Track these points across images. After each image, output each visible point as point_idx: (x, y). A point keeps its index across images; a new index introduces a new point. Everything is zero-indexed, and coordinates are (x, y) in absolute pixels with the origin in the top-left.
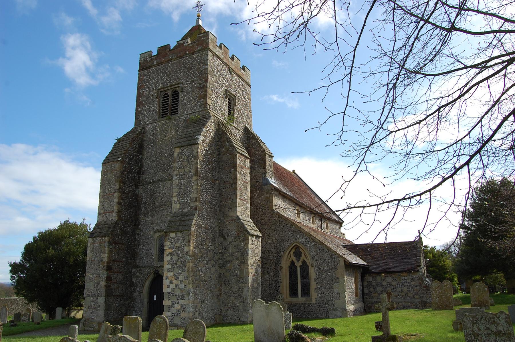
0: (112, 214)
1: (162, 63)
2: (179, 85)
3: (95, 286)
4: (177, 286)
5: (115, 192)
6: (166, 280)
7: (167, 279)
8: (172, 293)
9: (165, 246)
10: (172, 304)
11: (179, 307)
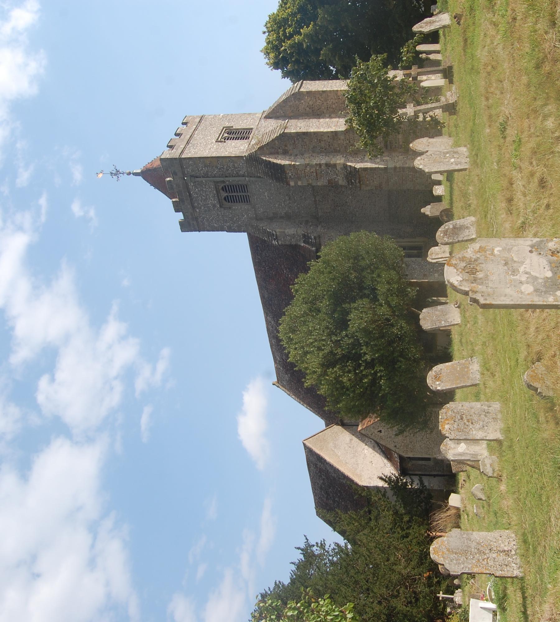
2: (225, 129)
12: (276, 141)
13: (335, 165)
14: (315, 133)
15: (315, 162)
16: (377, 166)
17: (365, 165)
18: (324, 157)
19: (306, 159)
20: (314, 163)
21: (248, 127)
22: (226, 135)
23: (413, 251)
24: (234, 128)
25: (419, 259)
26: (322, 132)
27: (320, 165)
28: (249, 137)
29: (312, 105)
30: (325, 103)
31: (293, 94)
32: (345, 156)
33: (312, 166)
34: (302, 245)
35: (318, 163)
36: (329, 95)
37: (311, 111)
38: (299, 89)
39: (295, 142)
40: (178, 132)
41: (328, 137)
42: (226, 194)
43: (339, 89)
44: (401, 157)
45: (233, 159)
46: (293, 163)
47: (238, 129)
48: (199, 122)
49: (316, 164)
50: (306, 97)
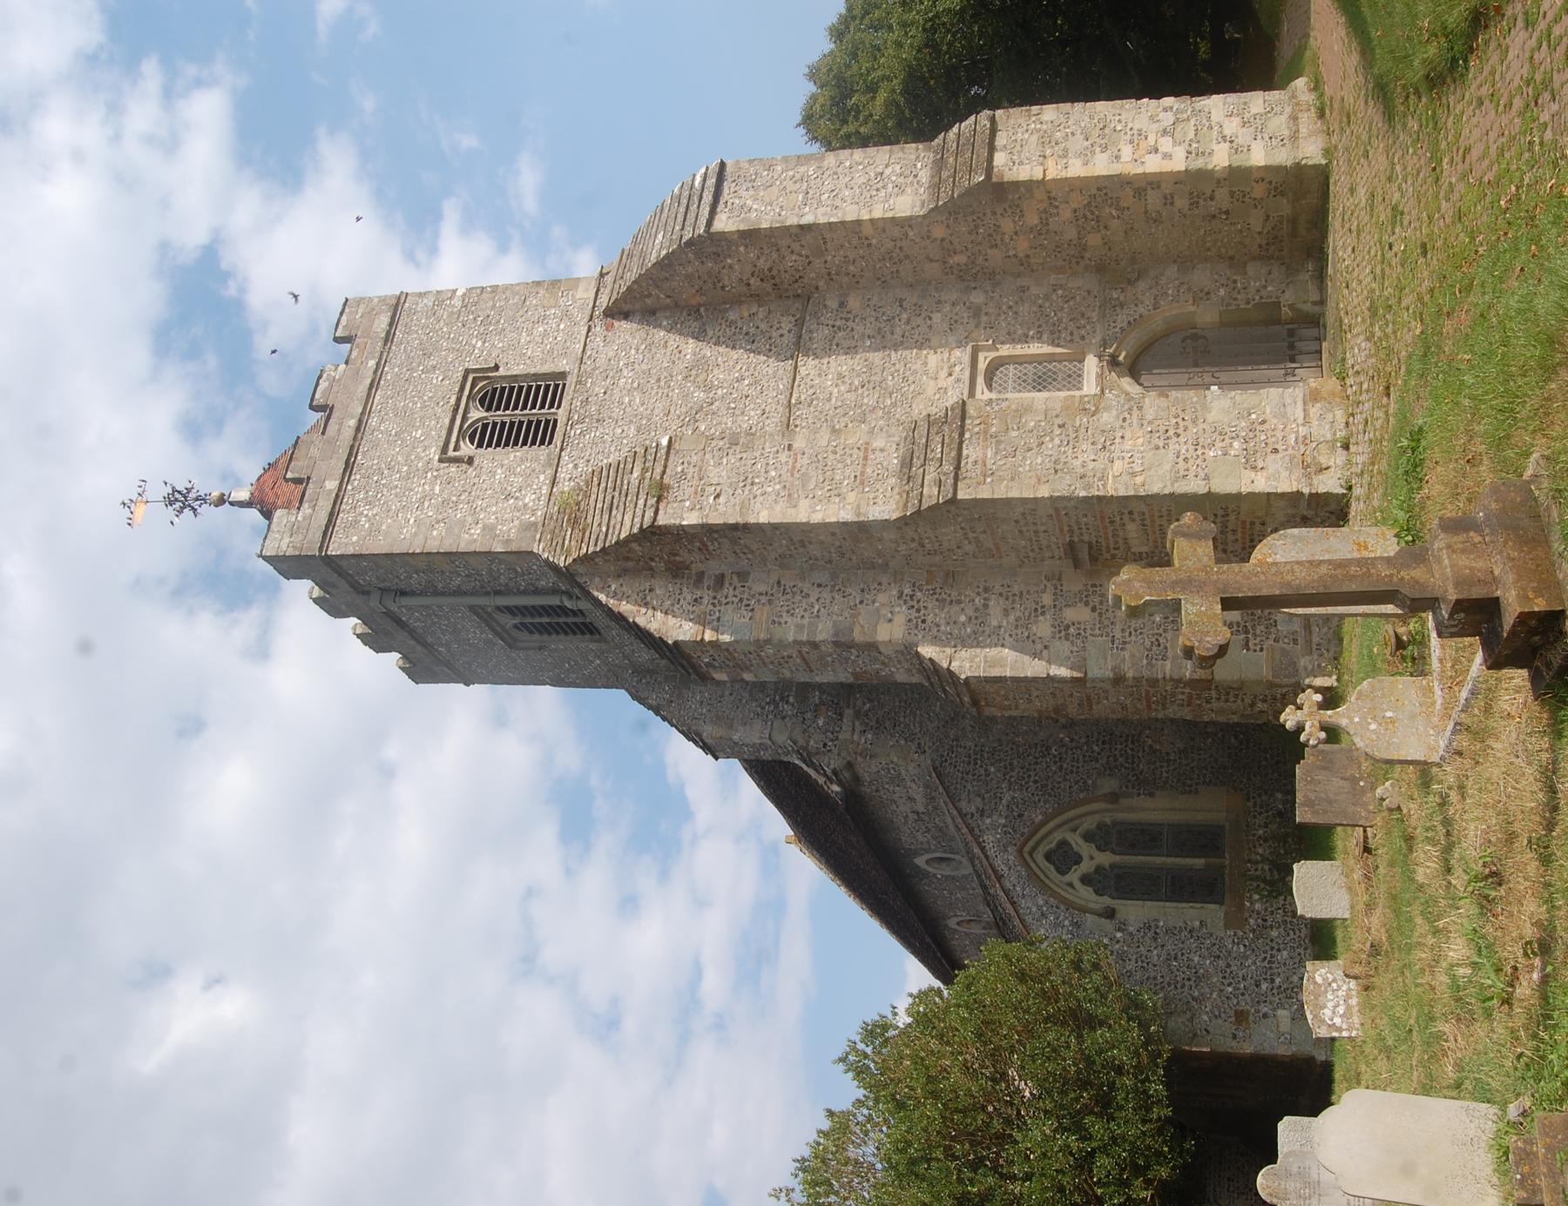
0: (874, 451)
1: (350, 455)
3: (1161, 445)
4: (1165, 132)
9: (1032, 176)
10: (1225, 141)
11: (1236, 121)
12: (634, 546)
13: (872, 647)
14: (775, 527)
15: (791, 631)
16: (1034, 668)
17: (992, 664)
18: (826, 595)
19: (758, 614)
20: (790, 640)
21: (547, 368)
22: (477, 414)
23: (1189, 861)
24: (502, 372)
25: (1213, 914)
26: (807, 524)
27: (815, 645)
28: (556, 421)
29: (770, 270)
30: (817, 263)
31: (690, 243)
32: (907, 591)
33: (782, 645)
34: (797, 762)
35: (804, 638)
36: (828, 236)
37: (768, 286)
38: (709, 223)
39: (705, 545)
41: (833, 534)
42: (517, 620)
45: (505, 557)
46: (709, 636)
47: (515, 378)
48: (386, 341)
49: (796, 642)
50: (742, 249)
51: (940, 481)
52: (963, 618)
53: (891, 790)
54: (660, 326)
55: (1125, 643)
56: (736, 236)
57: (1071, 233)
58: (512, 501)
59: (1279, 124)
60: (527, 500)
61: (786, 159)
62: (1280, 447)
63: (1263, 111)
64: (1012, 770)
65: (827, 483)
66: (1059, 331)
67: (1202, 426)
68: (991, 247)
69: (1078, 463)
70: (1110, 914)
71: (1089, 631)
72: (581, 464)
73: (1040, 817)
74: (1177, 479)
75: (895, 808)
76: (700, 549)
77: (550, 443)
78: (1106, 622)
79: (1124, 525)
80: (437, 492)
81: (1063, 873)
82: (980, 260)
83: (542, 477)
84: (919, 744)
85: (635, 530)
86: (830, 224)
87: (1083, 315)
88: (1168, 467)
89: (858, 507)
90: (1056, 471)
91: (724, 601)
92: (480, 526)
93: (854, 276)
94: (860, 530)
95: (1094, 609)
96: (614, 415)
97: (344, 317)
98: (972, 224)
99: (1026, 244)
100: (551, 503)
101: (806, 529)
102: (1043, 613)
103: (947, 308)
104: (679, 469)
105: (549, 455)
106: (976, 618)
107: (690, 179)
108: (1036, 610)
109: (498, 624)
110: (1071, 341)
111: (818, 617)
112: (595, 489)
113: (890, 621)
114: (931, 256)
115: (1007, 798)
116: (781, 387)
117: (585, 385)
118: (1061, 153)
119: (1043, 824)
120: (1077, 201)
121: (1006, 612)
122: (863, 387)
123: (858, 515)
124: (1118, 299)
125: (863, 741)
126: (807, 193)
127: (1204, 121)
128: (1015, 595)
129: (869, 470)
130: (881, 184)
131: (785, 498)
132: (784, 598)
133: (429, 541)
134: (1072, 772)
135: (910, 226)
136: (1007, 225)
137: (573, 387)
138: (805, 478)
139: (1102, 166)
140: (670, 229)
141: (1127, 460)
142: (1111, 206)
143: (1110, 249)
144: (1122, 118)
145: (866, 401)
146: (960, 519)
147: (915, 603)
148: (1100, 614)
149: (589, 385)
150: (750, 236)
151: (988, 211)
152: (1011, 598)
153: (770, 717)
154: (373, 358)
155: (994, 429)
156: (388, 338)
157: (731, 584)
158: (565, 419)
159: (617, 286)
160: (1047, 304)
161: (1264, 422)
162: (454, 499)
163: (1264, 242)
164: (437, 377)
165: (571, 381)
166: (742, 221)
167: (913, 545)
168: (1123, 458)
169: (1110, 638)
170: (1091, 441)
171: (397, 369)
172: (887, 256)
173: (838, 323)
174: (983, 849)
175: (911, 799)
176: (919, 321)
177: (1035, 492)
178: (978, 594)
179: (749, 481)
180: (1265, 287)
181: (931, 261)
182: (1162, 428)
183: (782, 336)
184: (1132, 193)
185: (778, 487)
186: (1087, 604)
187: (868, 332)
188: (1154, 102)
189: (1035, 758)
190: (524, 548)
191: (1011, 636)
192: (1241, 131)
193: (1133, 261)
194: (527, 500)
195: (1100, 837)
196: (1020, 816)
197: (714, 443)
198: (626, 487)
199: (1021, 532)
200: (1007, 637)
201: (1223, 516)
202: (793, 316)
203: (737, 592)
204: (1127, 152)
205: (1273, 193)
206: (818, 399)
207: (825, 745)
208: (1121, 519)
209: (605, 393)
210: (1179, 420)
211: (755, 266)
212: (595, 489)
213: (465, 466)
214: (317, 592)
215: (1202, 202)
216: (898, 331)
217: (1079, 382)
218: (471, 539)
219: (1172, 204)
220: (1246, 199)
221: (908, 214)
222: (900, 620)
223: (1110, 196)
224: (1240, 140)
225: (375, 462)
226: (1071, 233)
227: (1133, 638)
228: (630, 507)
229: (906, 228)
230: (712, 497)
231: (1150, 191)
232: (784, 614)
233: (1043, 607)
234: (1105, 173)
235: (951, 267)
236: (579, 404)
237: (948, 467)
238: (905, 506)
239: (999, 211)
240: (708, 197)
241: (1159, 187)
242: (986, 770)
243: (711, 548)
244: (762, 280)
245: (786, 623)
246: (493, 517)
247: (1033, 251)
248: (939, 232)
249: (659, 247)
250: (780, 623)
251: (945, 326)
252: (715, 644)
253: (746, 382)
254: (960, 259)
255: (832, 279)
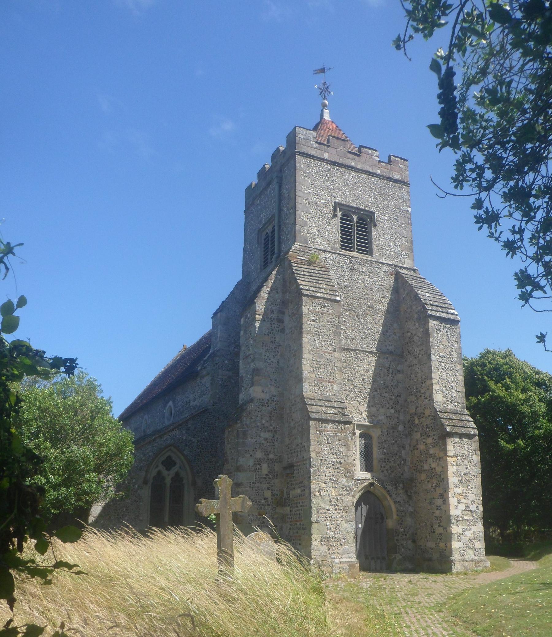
0: (332, 385)
3: (332, 503)
4: (467, 507)
5: (334, 351)
6: (452, 499)
7: (453, 497)
8: (461, 517)
9: (449, 451)
11: (472, 536)
12: (295, 286)
14: (301, 345)
21: (374, 247)
28: (351, 251)
29: (414, 341)
30: (415, 361)
31: (424, 308)
32: (275, 399)
40: (363, 150)
42: (269, 234)
43: (434, 381)
44: (268, 494)
45: (294, 230)
47: (371, 233)
50: (422, 330)
51: (318, 413)
52: (264, 422)
53: (199, 391)
54: (391, 295)
55: (253, 488)
56: (427, 327)
57: (426, 467)
58: (317, 233)
59: (470, 555)
60: (317, 239)
61: (460, 348)
62: (330, 552)
63: (476, 547)
64: (206, 442)
65: (319, 366)
66: (385, 462)
67: (340, 520)
68: (421, 434)
69: (325, 469)
70: (145, 482)
71: (258, 473)
72: (333, 262)
73: (186, 454)
74: (317, 510)
75: (192, 393)
76: (293, 313)
77: (342, 249)
78: (261, 480)
79: (300, 488)
80: (322, 201)
81: (163, 463)
82: (416, 429)
83: (327, 246)
84: (217, 403)
85: (301, 286)
86: (431, 367)
87: (392, 472)
88: (322, 505)
89: (309, 379)
90: (321, 460)
91: (272, 323)
92: (307, 220)
93: (411, 376)
94: (299, 379)
95: (267, 475)
96: (353, 276)
97: (399, 159)
98: (430, 426)
99: (422, 448)
100: (316, 250)
101: (300, 358)
102: (265, 454)
103: (396, 415)
104: (326, 305)
105: (337, 248)
106: (264, 427)
107: (453, 308)
108: (267, 452)
109: (268, 226)
110: (381, 467)
111: (265, 362)
112: (319, 269)
113: (263, 392)
114: (418, 409)
115: (194, 440)
116: (364, 346)
117: (367, 263)
118: (459, 463)
119: (183, 455)
120: (439, 469)
121: (266, 439)
122: (363, 380)
123: (305, 379)
124: (399, 486)
125: (219, 380)
126: (445, 357)
127: (472, 523)
128: (273, 443)
129: (324, 383)
130: (448, 388)
131: (313, 349)
132: (273, 347)
133: (300, 198)
134: (205, 466)
135: (429, 400)
136: (429, 441)
137: (365, 258)
138: (321, 357)
139: (453, 480)
140: (431, 299)
141: (326, 489)
142: (437, 484)
143: (420, 483)
144: (474, 489)
145: (357, 381)
146: (303, 421)
147: (270, 402)
148: (265, 478)
149: (366, 265)
150: (427, 333)
151: (435, 433)
152: (272, 441)
153: (229, 341)
154: (381, 172)
155: (339, 435)
156: (390, 179)
157: (279, 326)
158: (352, 255)
159: (409, 276)
160: (397, 457)
161: (341, 545)
162: (319, 209)
163: (422, 547)
164: (371, 200)
165: (369, 258)
166: (433, 330)
167: (293, 402)
168: (326, 487)
169: (255, 482)
170: (334, 474)
171: (376, 183)
172: (418, 390)
173: (391, 370)
174: (172, 430)
175: (195, 400)
176: (391, 404)
177: (313, 451)
178: (274, 428)
179: (320, 334)
180: (403, 547)
181: (416, 409)
182: (339, 504)
183: (386, 346)
184: (441, 492)
185: (318, 345)
186: (269, 472)
187: (387, 383)
188: (480, 502)
189: (211, 451)
190: (298, 238)
191: (256, 441)
192: (467, 538)
193: (415, 493)
194: (317, 239)
195: (177, 478)
196: (186, 445)
197: (337, 319)
198: (319, 282)
199: (298, 445)
200: (255, 440)
201: (303, 528)
202: (394, 351)
203: (276, 328)
204: (459, 490)
205: (441, 551)
206: (358, 361)
207: (217, 364)
208: (302, 486)
209: (363, 272)
210: (342, 510)
211: (415, 335)
212: (319, 269)
213: (332, 213)
214: (282, 149)
215: (438, 521)
216: (387, 395)
217: (364, 470)
218: (301, 216)
219: (437, 509)
220: (439, 540)
221: (434, 399)
222: (262, 396)
223: (441, 483)
224: (463, 537)
225: (336, 175)
226: (426, 467)
227: (254, 491)
228: (311, 284)
229: (429, 398)
230: (314, 318)
231: (442, 500)
232: (267, 348)
233: (268, 454)
234: (450, 481)
235: (413, 417)
236: (358, 261)
237: (324, 416)
238: (308, 398)
239: (435, 437)
240: (444, 315)
241: (444, 504)
242: (205, 431)
243: (294, 318)
244: (409, 338)
245: (263, 349)
246: (310, 225)
247: (419, 451)
248: (427, 412)
249: (424, 295)
250: (262, 346)
251: (388, 414)
252: (254, 320)
253: (366, 332)
254: (417, 421)
255: (409, 367)
